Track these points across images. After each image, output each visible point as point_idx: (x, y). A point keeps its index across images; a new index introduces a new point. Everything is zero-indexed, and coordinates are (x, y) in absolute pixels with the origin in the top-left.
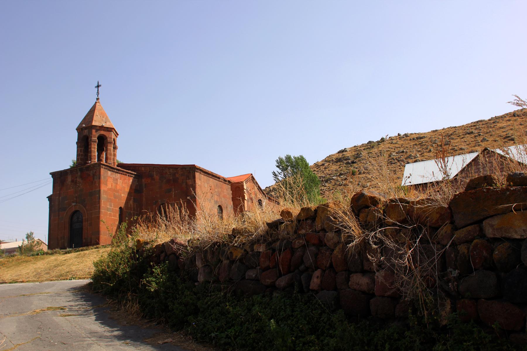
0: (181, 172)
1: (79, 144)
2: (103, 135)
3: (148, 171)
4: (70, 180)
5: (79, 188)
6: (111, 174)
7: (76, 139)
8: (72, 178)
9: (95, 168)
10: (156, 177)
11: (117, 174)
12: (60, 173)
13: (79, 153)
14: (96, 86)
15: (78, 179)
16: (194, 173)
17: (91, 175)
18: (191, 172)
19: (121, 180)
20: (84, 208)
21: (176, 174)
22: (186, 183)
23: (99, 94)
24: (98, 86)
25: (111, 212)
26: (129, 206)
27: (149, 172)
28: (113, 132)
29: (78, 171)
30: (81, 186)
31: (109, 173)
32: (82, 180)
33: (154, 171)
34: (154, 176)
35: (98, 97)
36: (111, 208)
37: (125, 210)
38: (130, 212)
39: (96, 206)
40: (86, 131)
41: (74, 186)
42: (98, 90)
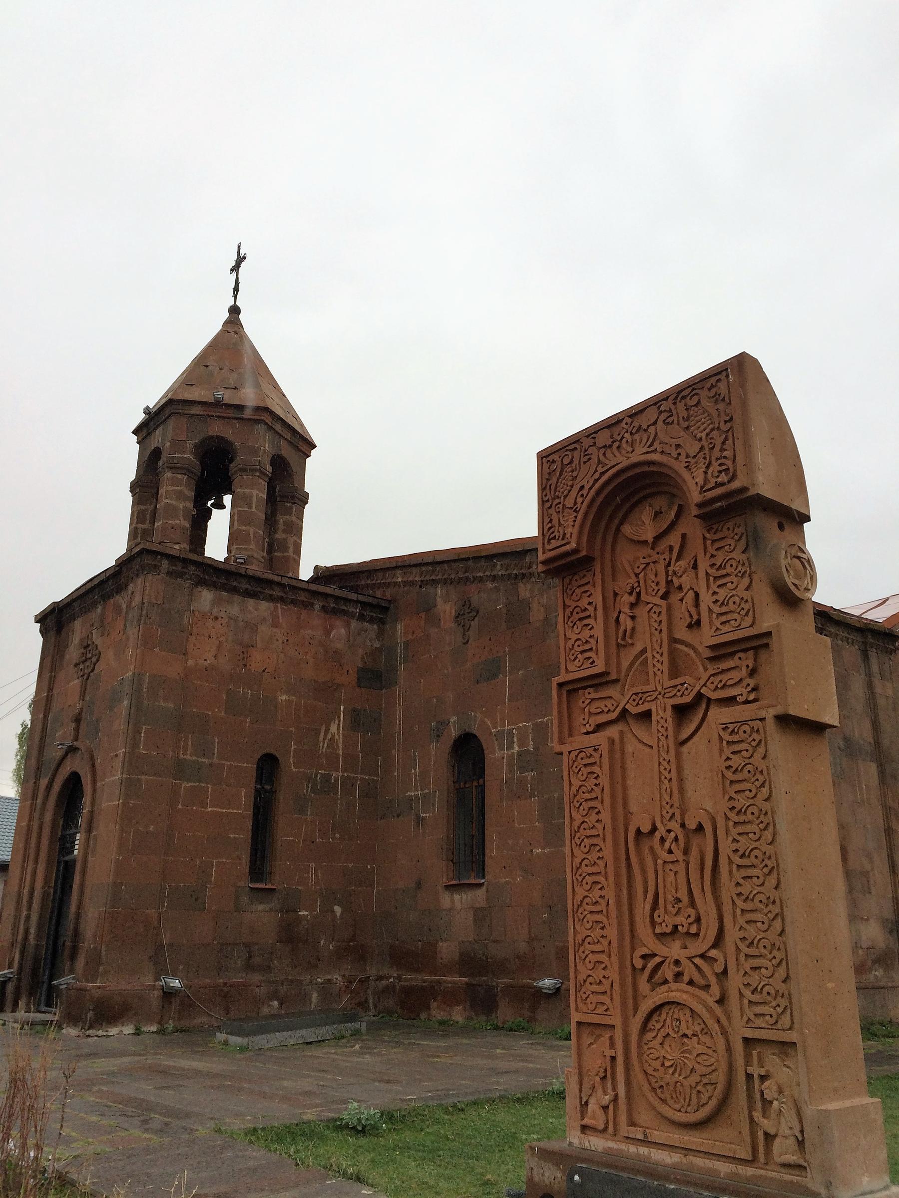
2: (221, 439)
6: (216, 602)
7: (130, 473)
11: (251, 602)
13: (134, 525)
17: (124, 606)
19: (274, 630)
25: (200, 781)
26: (323, 747)
28: (270, 428)
31: (206, 597)
34: (436, 606)
36: (206, 761)
37: (294, 770)
38: (326, 778)
39: (116, 755)
40: (157, 432)
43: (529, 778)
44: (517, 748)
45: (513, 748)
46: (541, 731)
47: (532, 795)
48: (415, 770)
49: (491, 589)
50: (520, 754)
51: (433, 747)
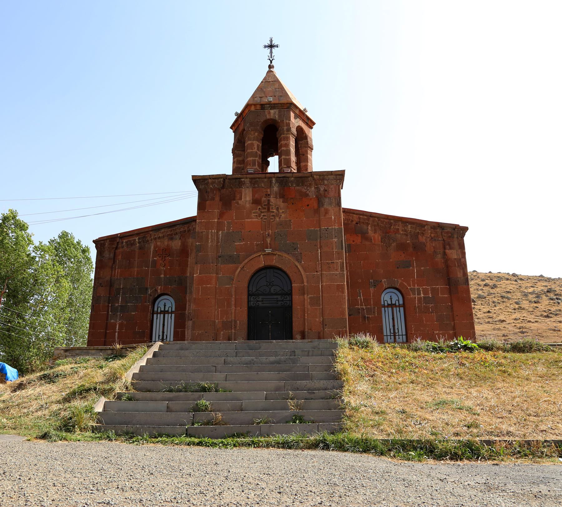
0: (431, 233)
1: (256, 134)
3: (354, 223)
4: (248, 199)
5: (277, 219)
8: (253, 196)
9: (326, 182)
10: (375, 236)
12: (222, 179)
14: (267, 45)
15: (272, 200)
16: (460, 239)
18: (456, 236)
20: (297, 264)
21: (420, 237)
22: (445, 254)
23: (273, 60)
24: (271, 46)
27: (357, 223)
29: (274, 182)
30: (283, 215)
32: (283, 202)
33: (368, 224)
35: (271, 62)
39: (333, 263)
40: (272, 111)
41: (263, 212)
42: (271, 52)
43: (430, 306)
44: (422, 295)
45: (421, 295)
46: (434, 291)
47: (431, 313)
48: (360, 297)
49: (403, 234)
50: (424, 298)
51: (372, 289)
